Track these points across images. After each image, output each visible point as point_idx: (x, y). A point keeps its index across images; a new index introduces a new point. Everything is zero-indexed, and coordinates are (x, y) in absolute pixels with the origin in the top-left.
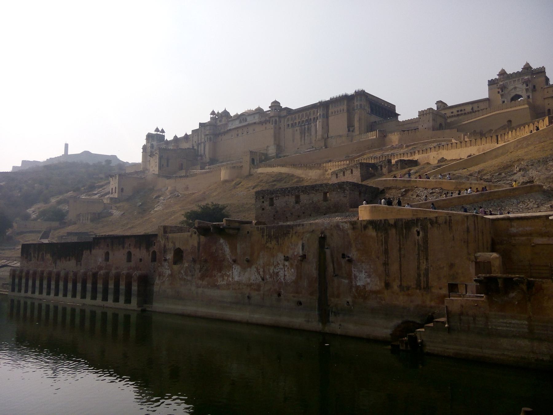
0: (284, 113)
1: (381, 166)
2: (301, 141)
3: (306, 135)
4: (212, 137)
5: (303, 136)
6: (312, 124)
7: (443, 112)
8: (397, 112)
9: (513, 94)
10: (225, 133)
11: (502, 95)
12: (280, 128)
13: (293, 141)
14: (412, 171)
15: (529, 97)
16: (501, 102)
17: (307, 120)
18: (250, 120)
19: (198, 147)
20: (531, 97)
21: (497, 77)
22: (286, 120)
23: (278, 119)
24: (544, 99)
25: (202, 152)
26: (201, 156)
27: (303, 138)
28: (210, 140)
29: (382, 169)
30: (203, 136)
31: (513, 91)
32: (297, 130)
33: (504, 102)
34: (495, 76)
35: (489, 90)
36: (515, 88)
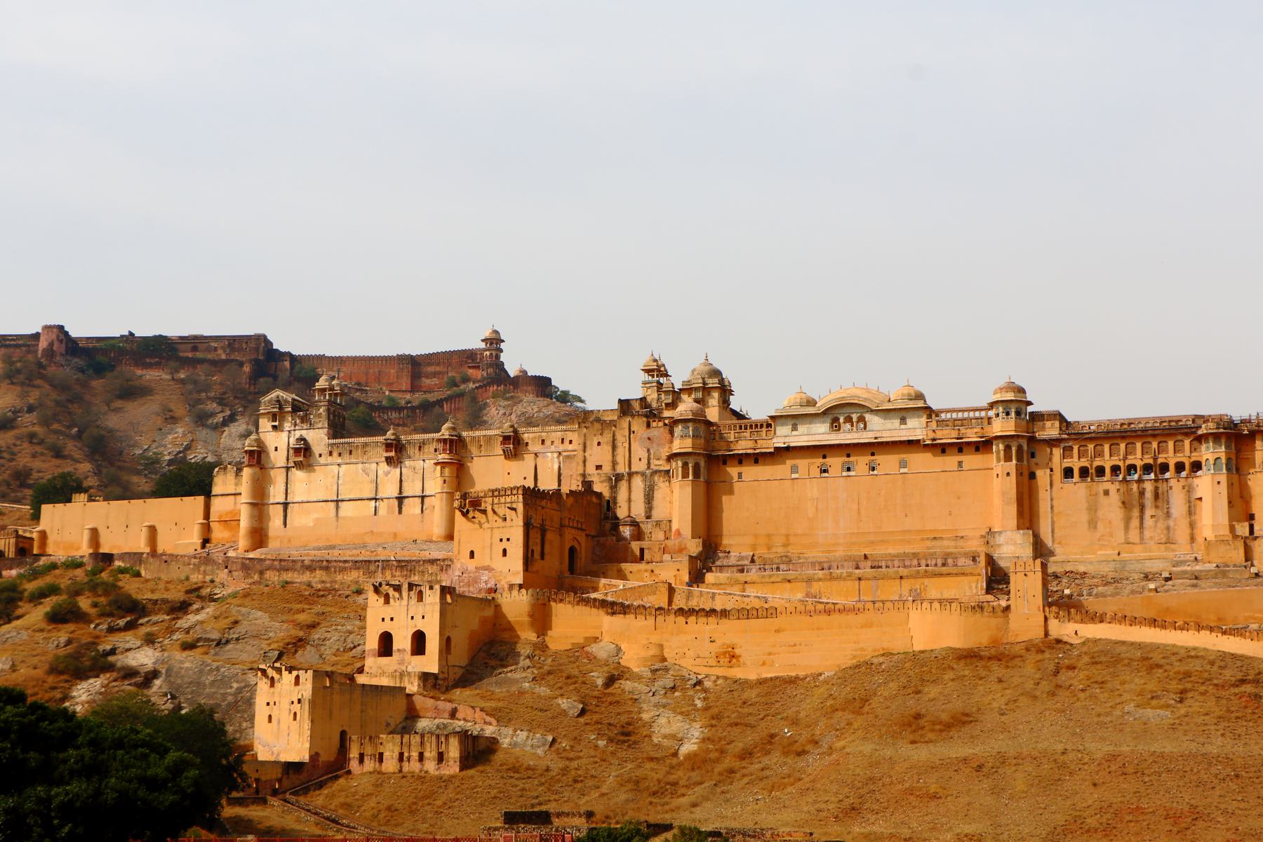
0: (1051, 430)
2: (1127, 528)
3: (1149, 512)
5: (1136, 513)
10: (757, 458)
13: (1093, 524)
17: (1147, 468)
18: (881, 430)
19: (614, 488)
22: (1057, 452)
23: (1025, 448)
25: (638, 510)
26: (635, 524)
27: (1135, 523)
28: (697, 474)
30: (639, 451)
32: (1106, 493)
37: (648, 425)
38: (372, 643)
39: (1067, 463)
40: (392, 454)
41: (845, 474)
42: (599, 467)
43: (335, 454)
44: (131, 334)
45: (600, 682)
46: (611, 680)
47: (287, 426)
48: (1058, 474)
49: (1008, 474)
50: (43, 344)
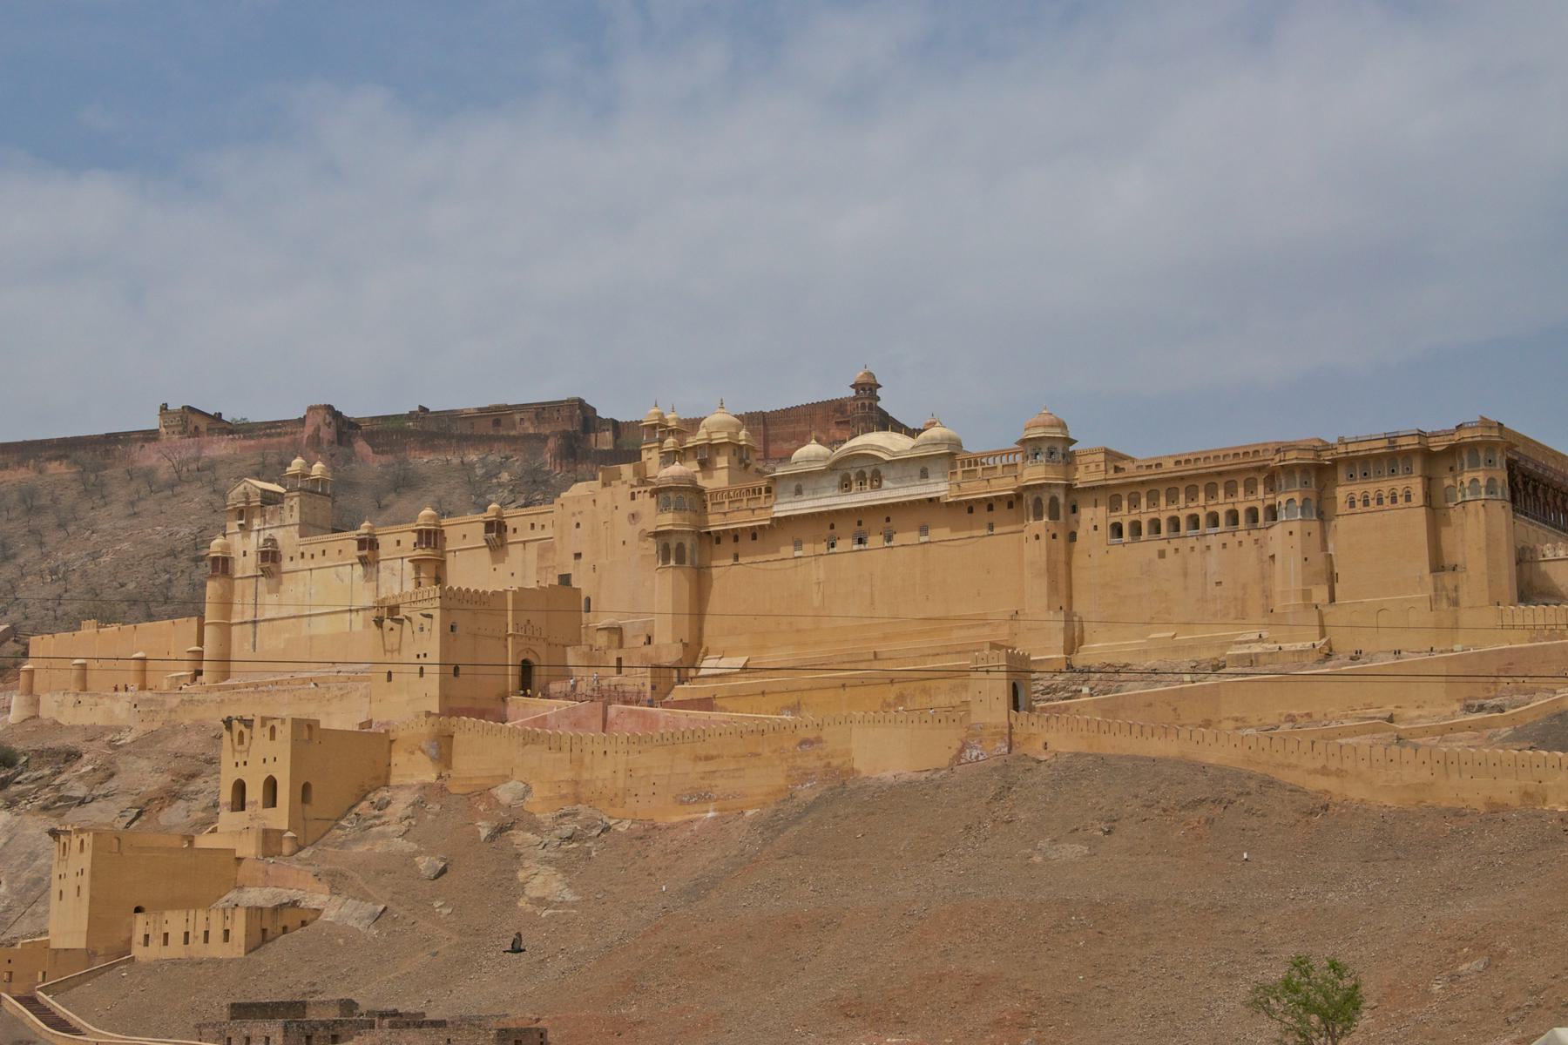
4: (688, 544)
6: (1241, 535)
12: (1072, 537)
23: (1062, 500)
28: (680, 560)
32: (1162, 554)
37: (633, 497)
38: (226, 796)
39: (1115, 518)
40: (365, 552)
41: (856, 547)
42: (578, 556)
43: (308, 556)
44: (423, 409)
45: (484, 833)
46: (501, 830)
47: (257, 523)
48: (1104, 530)
49: (1037, 537)
50: (308, 430)
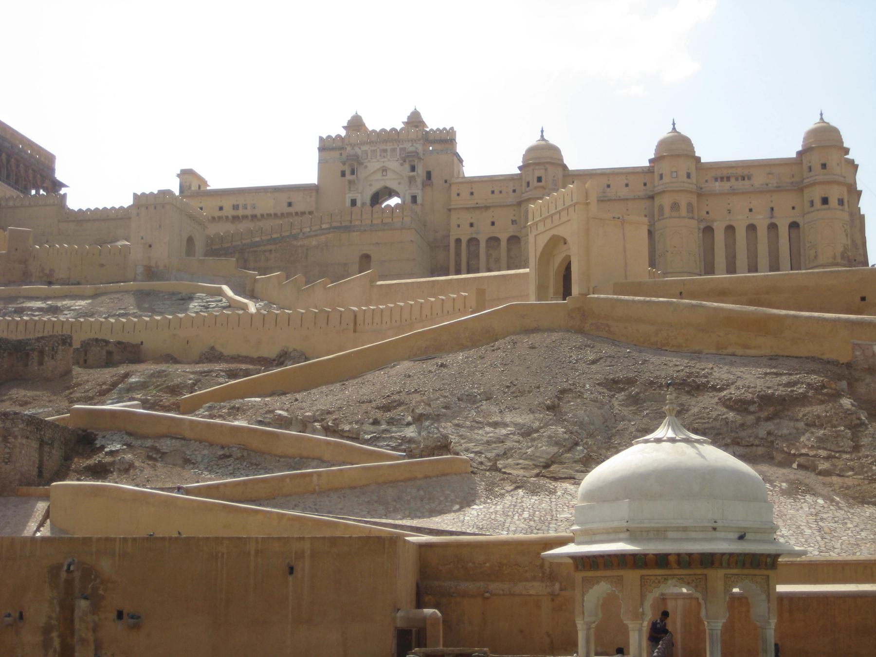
1: (41, 353)
7: (195, 204)
8: (59, 175)
9: (377, 187)
11: (350, 182)
14: (133, 380)
15: (414, 199)
16: (348, 203)
20: (419, 200)
21: (343, 133)
24: (450, 210)
29: (41, 363)
31: (379, 176)
33: (354, 203)
34: (337, 129)
35: (321, 162)
36: (384, 170)
